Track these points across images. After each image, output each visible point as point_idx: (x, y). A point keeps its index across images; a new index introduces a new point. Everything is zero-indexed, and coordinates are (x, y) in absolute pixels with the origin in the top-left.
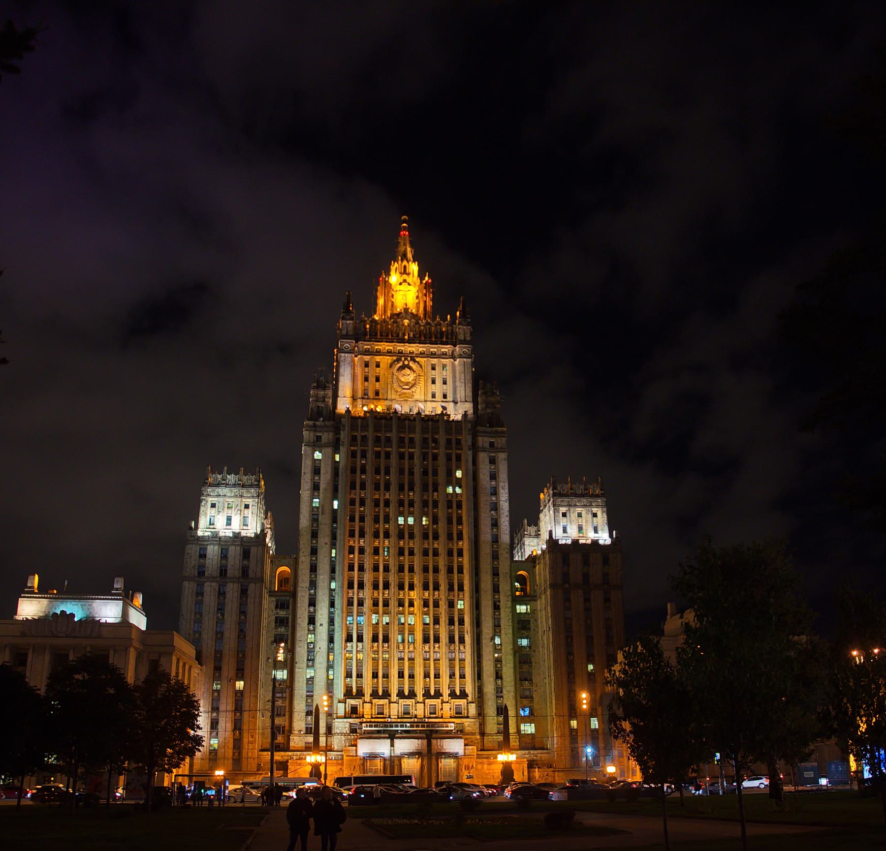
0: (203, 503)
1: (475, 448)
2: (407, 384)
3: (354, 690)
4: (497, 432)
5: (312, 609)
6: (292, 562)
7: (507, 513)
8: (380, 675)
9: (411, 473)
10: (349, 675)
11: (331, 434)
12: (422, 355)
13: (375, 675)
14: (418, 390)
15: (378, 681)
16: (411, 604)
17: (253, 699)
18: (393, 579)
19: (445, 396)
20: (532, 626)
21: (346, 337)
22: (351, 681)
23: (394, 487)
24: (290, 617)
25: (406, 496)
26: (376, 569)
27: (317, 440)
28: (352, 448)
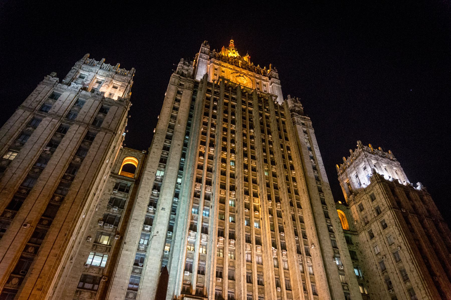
3: (194, 288)
4: (305, 118)
5: (155, 192)
6: (141, 156)
8: (226, 273)
10: (189, 268)
13: (219, 275)
15: (222, 283)
17: (52, 259)
22: (191, 277)
24: (128, 200)
25: (249, 131)
28: (207, 95)
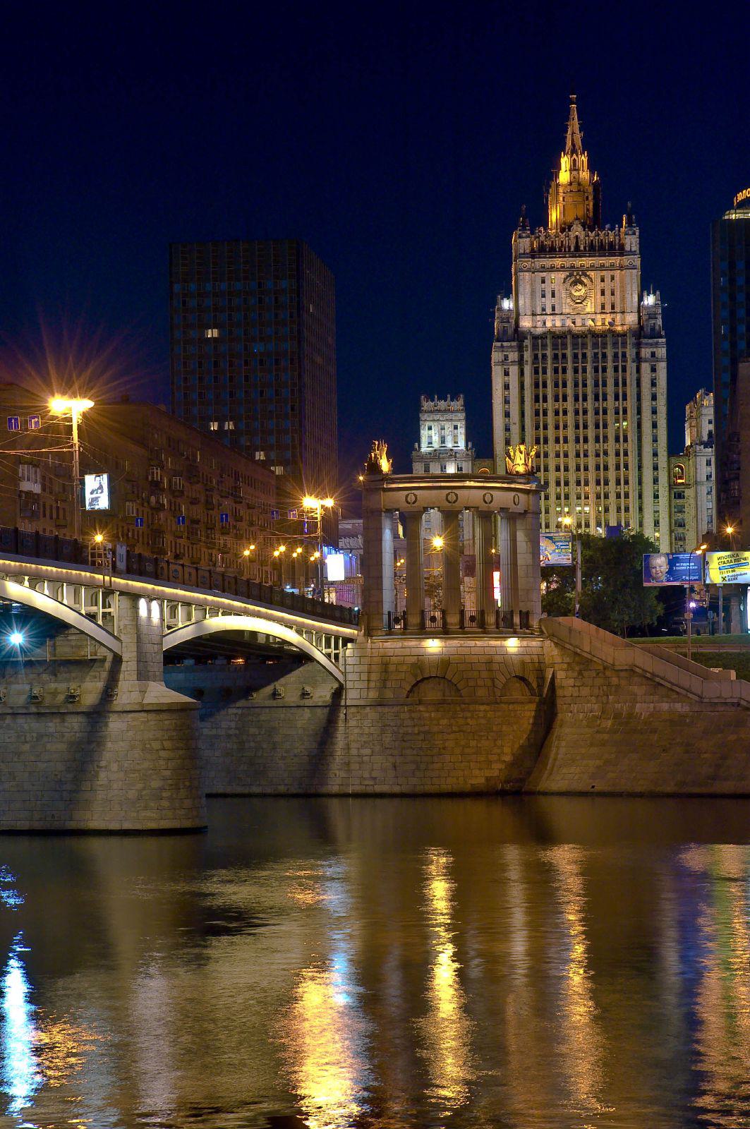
0: (422, 427)
1: (638, 359)
2: (579, 297)
7: (665, 416)
9: (585, 385)
11: (516, 353)
12: (592, 268)
14: (589, 303)
16: (587, 498)
18: (572, 477)
19: (613, 307)
20: (686, 510)
21: (524, 255)
23: (570, 399)
26: (558, 469)
27: (505, 359)
